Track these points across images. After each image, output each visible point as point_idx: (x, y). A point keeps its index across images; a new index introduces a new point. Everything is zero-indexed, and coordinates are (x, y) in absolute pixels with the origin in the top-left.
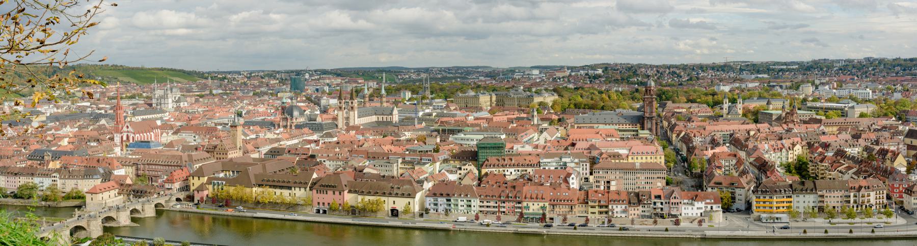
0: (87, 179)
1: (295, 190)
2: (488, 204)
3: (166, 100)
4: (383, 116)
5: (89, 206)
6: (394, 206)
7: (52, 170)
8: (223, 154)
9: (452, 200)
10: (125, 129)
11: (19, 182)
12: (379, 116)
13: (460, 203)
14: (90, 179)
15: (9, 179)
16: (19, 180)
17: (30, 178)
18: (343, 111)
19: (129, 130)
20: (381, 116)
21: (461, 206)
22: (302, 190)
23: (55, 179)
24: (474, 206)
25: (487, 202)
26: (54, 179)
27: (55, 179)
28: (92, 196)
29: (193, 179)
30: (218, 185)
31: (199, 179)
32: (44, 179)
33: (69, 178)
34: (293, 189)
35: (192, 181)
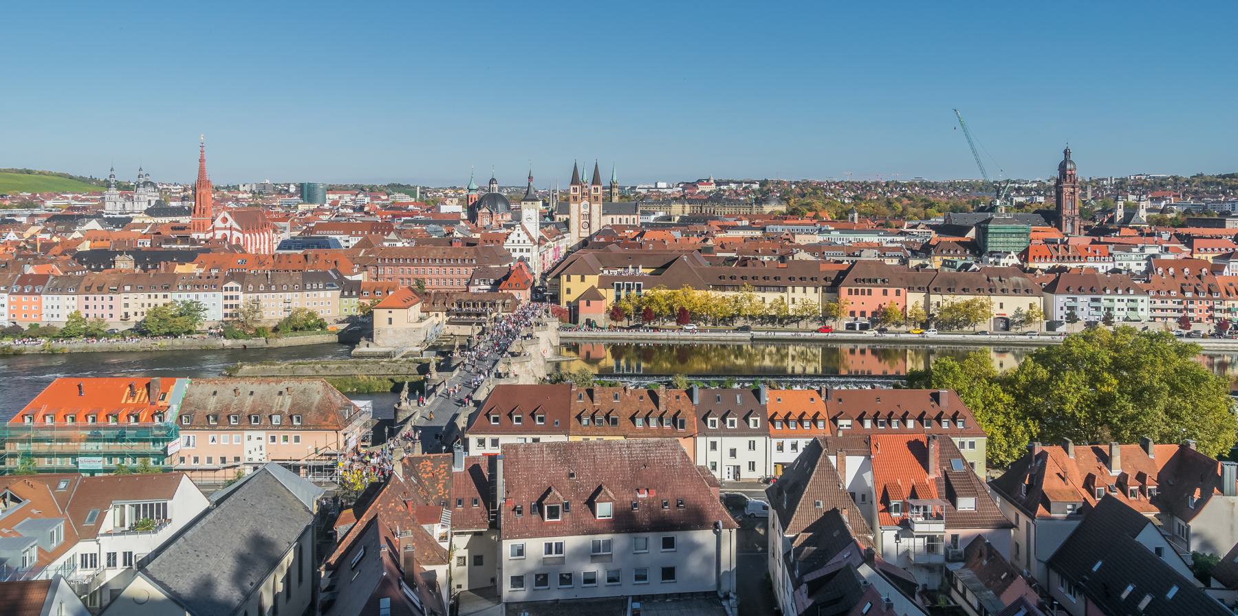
0: (312, 289)
1: (793, 291)
2: (1164, 306)
3: (136, 203)
4: (621, 216)
5: (381, 336)
6: (1001, 312)
7: (217, 277)
8: (521, 250)
9: (1103, 301)
10: (218, 223)
11: (127, 305)
12: (614, 217)
13: (1117, 305)
14: (318, 289)
15: (91, 302)
16: (87, 303)
17: (160, 295)
18: (579, 203)
19: (228, 225)
20: (619, 217)
21: (1119, 309)
22: (810, 290)
23: (234, 293)
24: (1142, 310)
25: (1162, 302)
26: (229, 293)
27: (234, 293)
28: (390, 316)
29: (569, 280)
30: (629, 289)
31: (583, 280)
32: (201, 295)
33: (268, 289)
34: (790, 289)
35: (565, 284)
